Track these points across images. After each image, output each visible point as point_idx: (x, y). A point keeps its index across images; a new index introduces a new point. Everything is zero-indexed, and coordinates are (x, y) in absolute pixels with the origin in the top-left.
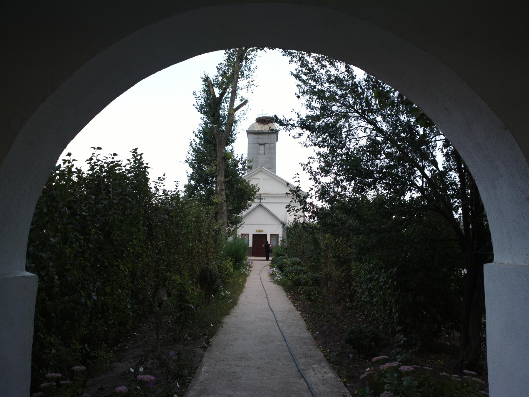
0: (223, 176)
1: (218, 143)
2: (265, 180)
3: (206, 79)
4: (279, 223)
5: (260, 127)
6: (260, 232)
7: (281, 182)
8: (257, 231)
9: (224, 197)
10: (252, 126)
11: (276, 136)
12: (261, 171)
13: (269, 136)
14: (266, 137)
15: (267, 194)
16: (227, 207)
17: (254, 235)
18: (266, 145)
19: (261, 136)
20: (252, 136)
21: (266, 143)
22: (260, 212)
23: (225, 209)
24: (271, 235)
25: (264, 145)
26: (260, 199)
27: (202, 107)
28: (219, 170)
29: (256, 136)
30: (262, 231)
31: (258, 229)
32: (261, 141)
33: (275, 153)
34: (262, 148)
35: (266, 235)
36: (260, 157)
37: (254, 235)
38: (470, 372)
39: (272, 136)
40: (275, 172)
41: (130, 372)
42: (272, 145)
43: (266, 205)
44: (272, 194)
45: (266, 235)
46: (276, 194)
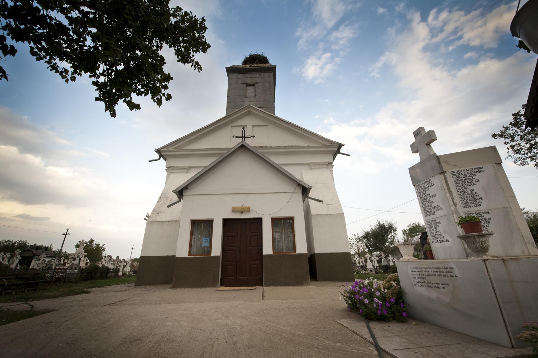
2: (256, 128)
6: (242, 212)
8: (234, 210)
11: (272, 74)
13: (262, 75)
17: (226, 222)
18: (256, 85)
19: (249, 75)
20: (234, 76)
21: (256, 83)
24: (276, 221)
25: (253, 85)
29: (241, 76)
30: (248, 210)
31: (238, 205)
32: (248, 81)
34: (251, 89)
35: (259, 221)
37: (226, 222)
40: (273, 111)
42: (267, 84)
45: (259, 221)
46: (278, 147)
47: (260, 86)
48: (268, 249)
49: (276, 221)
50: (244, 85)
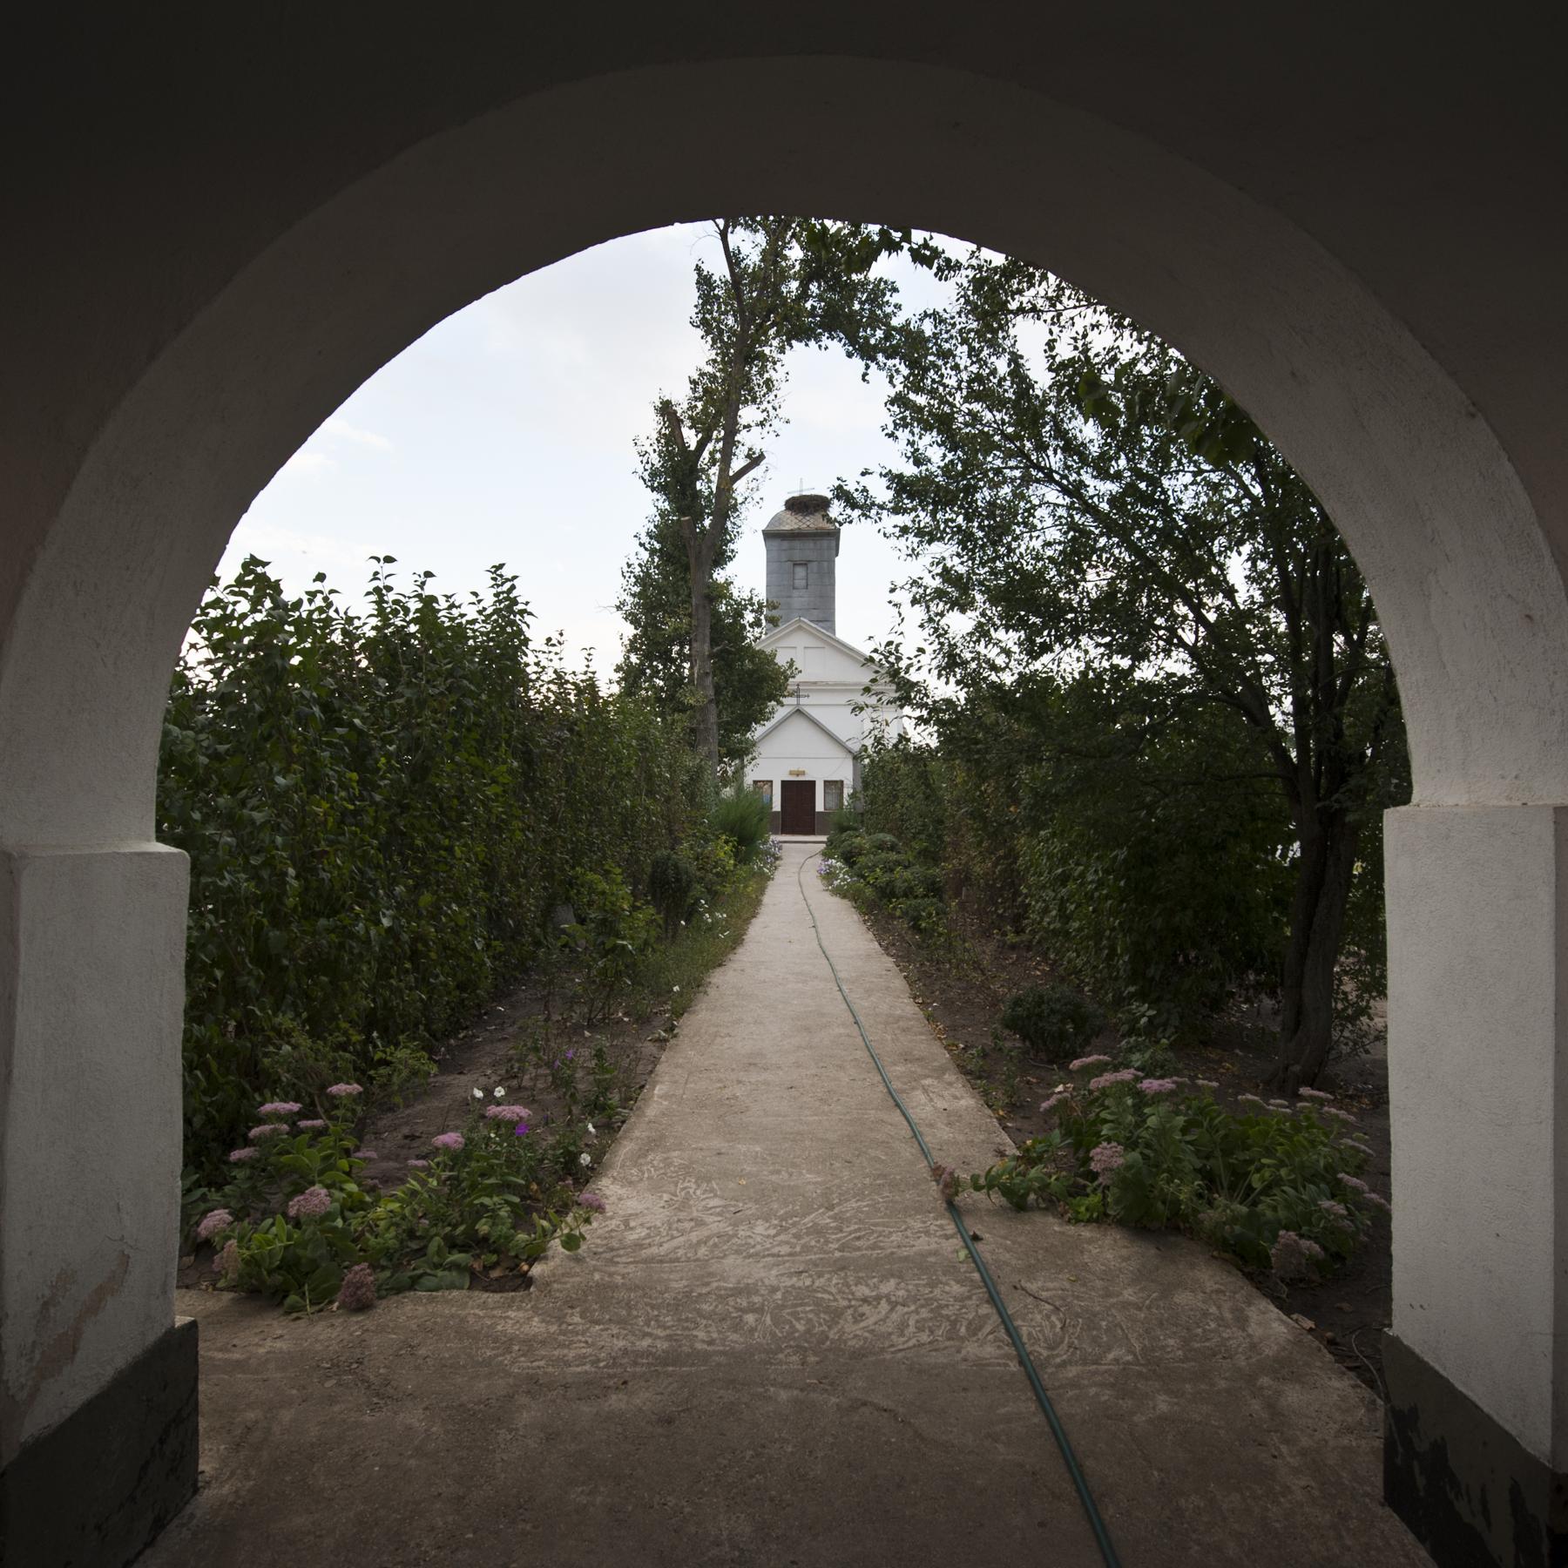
0: (708, 640)
1: (692, 561)
3: (666, 409)
4: (841, 754)
5: (792, 523)
7: (847, 655)
8: (791, 773)
9: (711, 692)
10: (777, 519)
11: (834, 543)
12: (800, 628)
14: (810, 544)
15: (815, 683)
16: (719, 716)
17: (784, 783)
18: (809, 565)
19: (797, 544)
20: (775, 543)
22: (799, 728)
23: (712, 720)
24: (827, 783)
25: (805, 564)
26: (798, 696)
27: (654, 474)
28: (696, 627)
29: (785, 544)
30: (803, 773)
32: (797, 556)
33: (833, 585)
34: (800, 572)
35: (812, 784)
36: (796, 593)
37: (784, 783)
38: (1316, 1093)
39: (825, 543)
40: (834, 633)
41: (473, 1097)
42: (826, 564)
43: (814, 713)
44: (827, 684)
45: (812, 784)
47: (813, 566)
48: (820, 807)
49: (827, 783)
50: (791, 564)
